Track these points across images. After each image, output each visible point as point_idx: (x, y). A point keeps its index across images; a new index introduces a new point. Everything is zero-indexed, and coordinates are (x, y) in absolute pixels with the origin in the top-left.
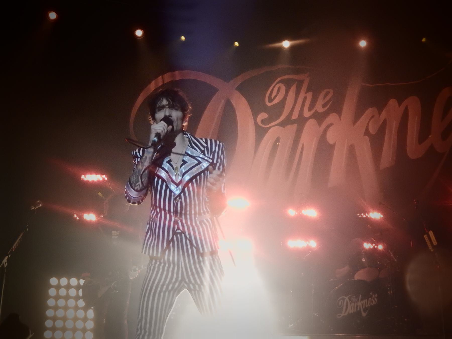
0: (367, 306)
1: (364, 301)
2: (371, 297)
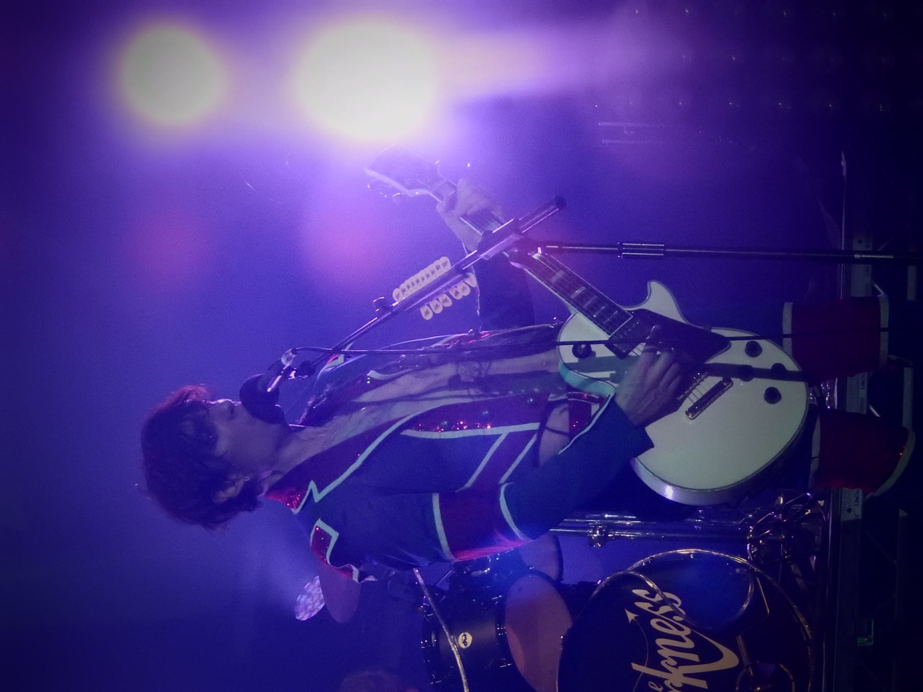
0: (690, 644)
1: (664, 652)
2: (645, 617)
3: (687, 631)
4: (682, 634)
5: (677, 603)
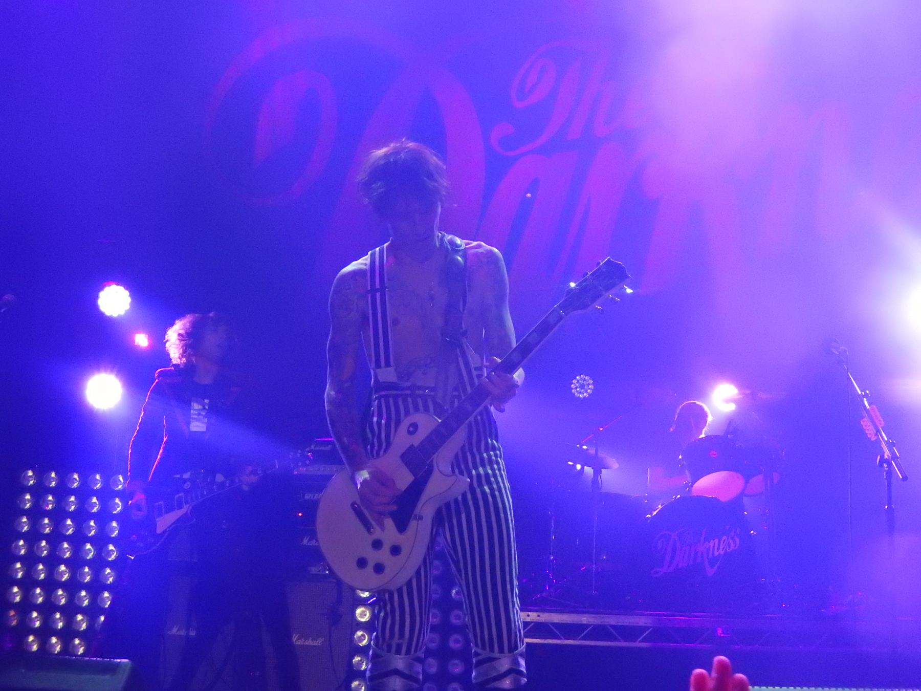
0: (716, 554)
1: (712, 544)
3: (722, 553)
4: (721, 550)
5: (735, 546)
